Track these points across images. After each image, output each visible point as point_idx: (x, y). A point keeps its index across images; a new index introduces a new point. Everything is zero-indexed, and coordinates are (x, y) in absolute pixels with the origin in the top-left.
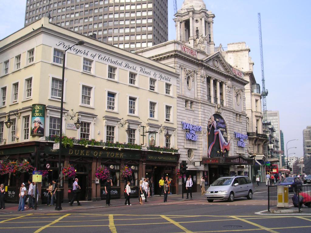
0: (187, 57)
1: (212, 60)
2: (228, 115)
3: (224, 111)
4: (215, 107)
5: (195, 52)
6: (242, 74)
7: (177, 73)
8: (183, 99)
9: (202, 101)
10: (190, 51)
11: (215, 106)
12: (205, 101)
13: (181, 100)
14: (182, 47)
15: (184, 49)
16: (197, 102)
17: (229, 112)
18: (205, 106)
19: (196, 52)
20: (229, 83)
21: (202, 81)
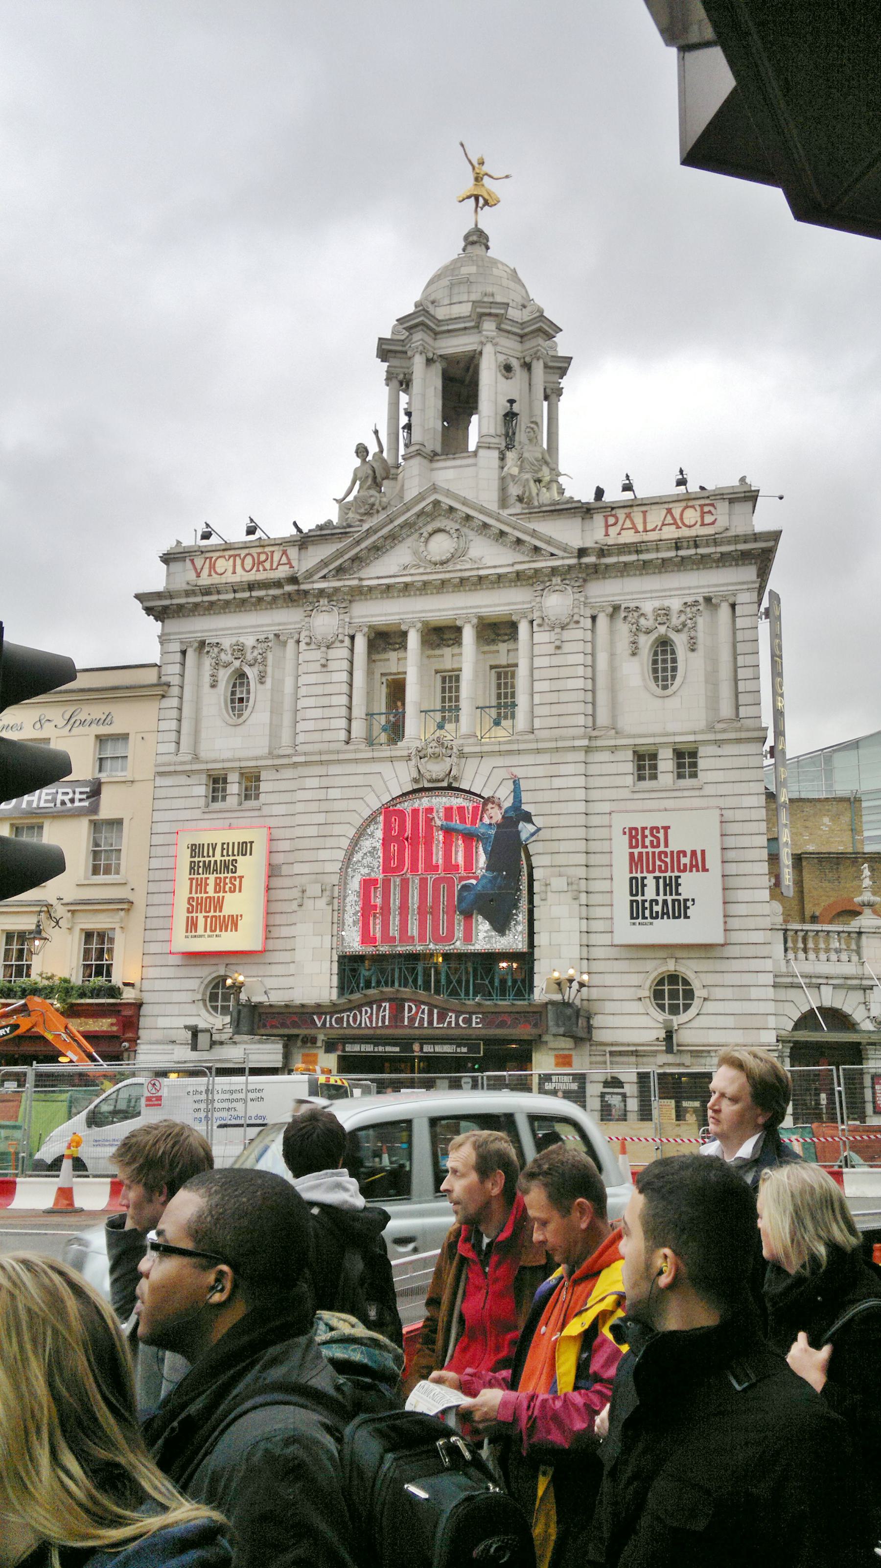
0: (206, 598)
1: (409, 542)
2: (540, 771)
3: (488, 763)
4: (409, 758)
5: (284, 553)
6: (723, 507)
7: (164, 679)
8: (189, 774)
9: (305, 754)
10: (249, 561)
11: (405, 753)
12: (333, 746)
13: (182, 780)
14: (199, 567)
15: (212, 567)
16: (277, 768)
17: (545, 758)
18: (334, 769)
19: (293, 552)
20: (557, 602)
21: (317, 667)
